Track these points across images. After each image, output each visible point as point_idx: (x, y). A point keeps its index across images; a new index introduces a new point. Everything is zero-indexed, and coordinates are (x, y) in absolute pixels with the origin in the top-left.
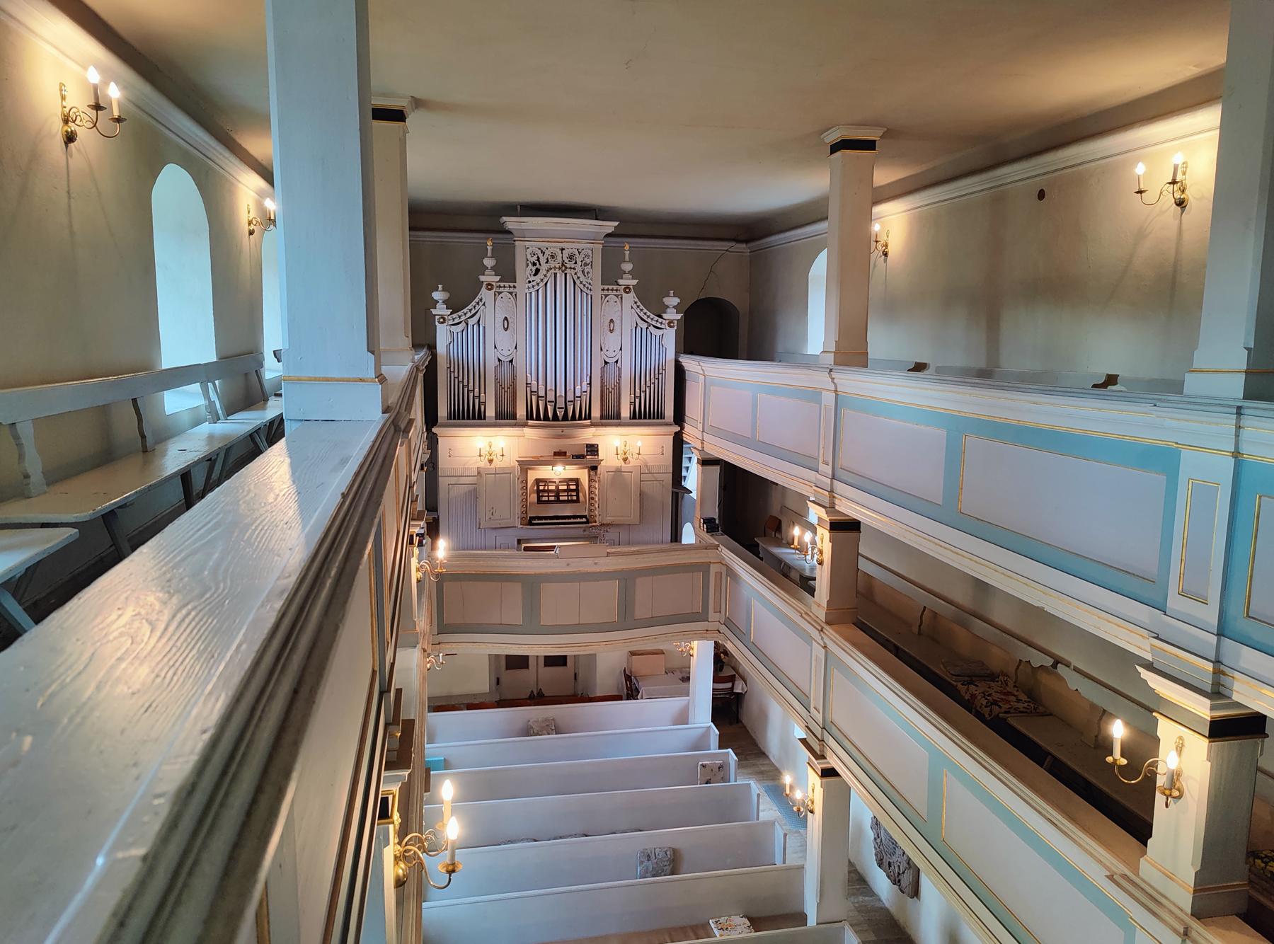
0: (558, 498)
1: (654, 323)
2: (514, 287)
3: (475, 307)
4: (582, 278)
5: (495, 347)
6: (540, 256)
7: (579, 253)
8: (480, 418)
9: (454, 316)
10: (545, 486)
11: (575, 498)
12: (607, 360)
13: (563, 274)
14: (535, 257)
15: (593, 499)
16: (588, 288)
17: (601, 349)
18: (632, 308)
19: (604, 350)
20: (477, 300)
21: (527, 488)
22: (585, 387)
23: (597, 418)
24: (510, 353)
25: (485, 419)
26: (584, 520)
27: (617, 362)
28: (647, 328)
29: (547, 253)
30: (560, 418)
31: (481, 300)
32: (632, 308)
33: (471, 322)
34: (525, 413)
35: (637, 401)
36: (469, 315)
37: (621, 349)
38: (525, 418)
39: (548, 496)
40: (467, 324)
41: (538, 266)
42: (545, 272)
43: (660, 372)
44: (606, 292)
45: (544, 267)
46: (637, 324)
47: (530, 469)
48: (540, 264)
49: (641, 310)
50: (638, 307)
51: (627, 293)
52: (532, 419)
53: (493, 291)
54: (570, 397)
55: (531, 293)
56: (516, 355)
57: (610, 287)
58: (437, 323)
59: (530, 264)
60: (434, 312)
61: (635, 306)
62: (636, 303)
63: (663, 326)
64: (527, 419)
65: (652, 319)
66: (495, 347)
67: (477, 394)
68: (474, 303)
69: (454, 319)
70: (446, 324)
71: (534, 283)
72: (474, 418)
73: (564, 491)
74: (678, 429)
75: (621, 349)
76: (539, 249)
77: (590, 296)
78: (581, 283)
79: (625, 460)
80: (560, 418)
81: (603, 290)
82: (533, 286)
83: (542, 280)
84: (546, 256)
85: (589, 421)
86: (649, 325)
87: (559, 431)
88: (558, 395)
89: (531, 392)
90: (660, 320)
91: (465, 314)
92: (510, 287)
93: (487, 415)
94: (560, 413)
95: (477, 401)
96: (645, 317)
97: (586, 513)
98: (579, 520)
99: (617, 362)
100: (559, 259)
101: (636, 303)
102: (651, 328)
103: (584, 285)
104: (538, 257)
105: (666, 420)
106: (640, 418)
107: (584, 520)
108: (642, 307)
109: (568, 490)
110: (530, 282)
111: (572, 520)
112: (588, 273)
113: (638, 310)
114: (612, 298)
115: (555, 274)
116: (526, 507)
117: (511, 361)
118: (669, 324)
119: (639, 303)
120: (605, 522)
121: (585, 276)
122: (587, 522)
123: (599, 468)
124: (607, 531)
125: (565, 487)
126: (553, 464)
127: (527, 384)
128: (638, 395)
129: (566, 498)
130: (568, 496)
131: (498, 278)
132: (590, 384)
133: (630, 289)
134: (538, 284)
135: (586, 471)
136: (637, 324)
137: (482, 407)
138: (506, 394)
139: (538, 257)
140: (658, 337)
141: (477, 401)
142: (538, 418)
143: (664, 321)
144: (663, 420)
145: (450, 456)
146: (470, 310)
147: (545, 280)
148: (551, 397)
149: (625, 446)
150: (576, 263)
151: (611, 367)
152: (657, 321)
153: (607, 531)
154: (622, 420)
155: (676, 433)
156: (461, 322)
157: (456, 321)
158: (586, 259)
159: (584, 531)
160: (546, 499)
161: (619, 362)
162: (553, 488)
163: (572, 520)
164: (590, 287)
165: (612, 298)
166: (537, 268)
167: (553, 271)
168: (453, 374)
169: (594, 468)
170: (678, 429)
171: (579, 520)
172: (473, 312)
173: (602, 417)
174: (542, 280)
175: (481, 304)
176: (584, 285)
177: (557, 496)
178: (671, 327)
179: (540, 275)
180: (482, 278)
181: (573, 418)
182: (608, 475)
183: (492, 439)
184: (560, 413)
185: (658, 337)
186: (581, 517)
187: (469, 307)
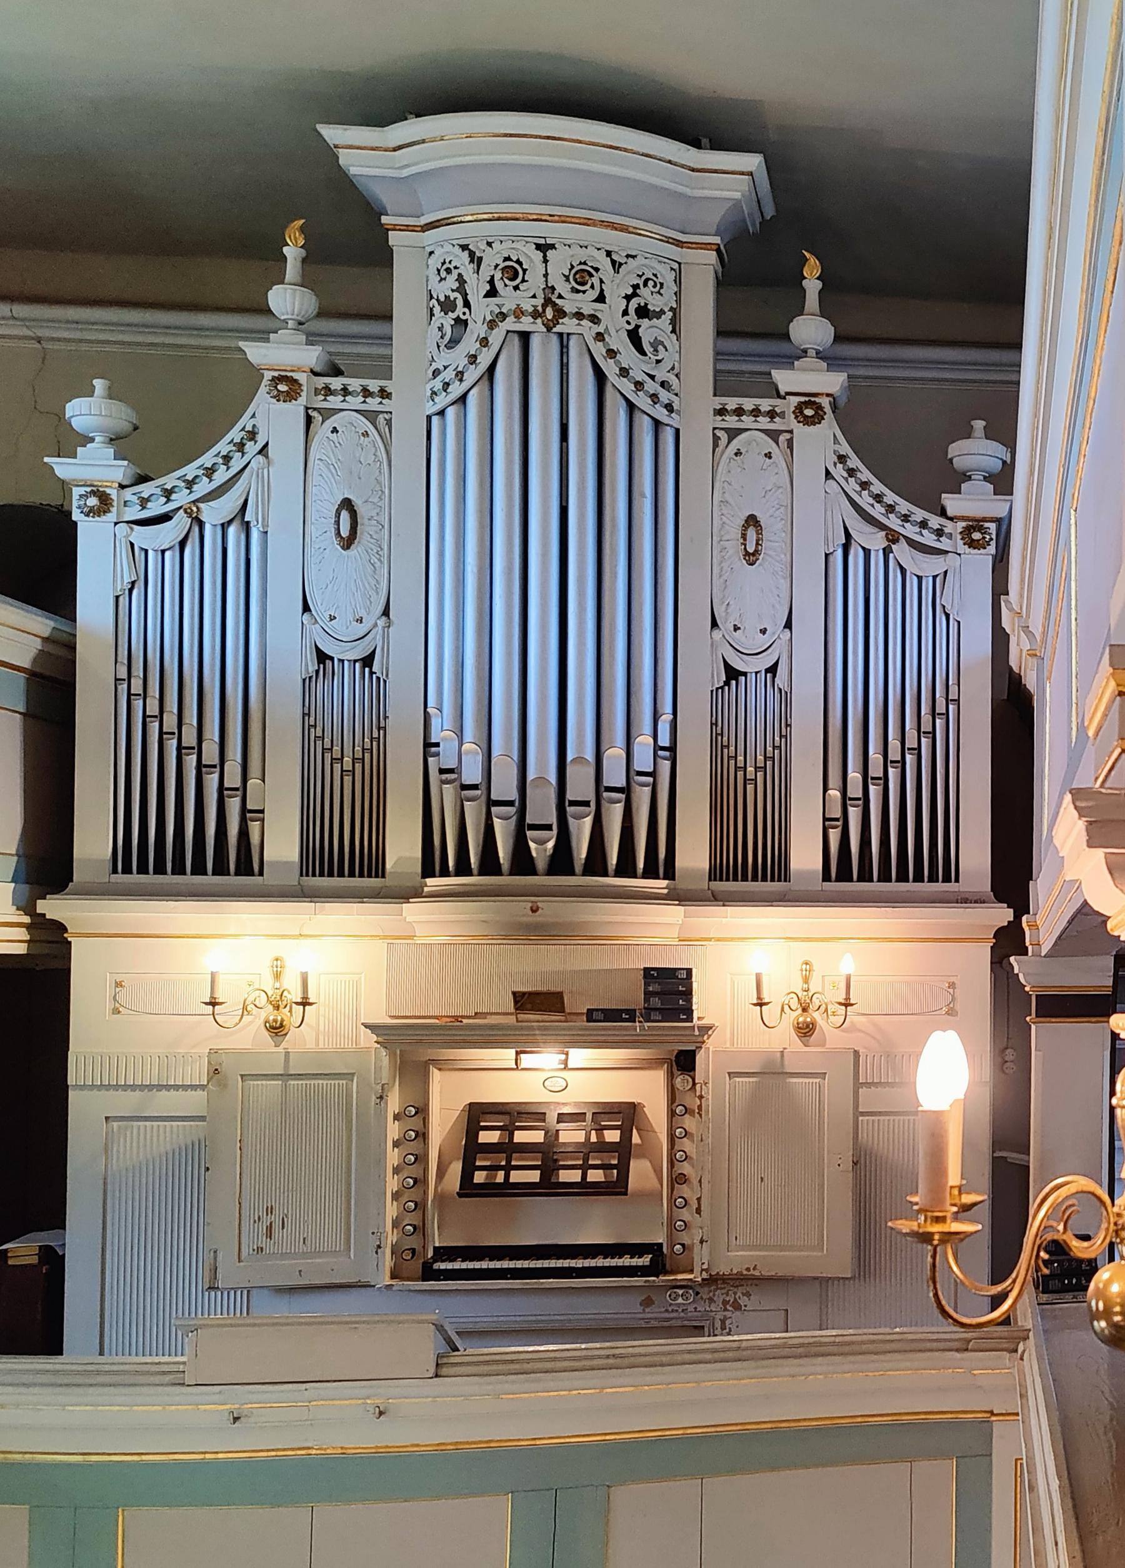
1: (910, 531)
2: (384, 394)
3: (227, 459)
4: (628, 355)
5: (306, 608)
6: (468, 271)
7: (616, 266)
8: (245, 867)
9: (146, 489)
12: (738, 664)
13: (555, 340)
14: (451, 282)
15: (681, 1179)
16: (654, 397)
17: (714, 624)
18: (828, 473)
19: (726, 625)
20: (235, 434)
21: (422, 1135)
22: (643, 760)
23: (691, 874)
24: (362, 629)
25: (261, 874)
26: (645, 1260)
27: (773, 670)
28: (887, 551)
29: (492, 258)
30: (541, 864)
31: (252, 435)
32: (828, 473)
33: (213, 514)
34: (419, 854)
35: (854, 814)
36: (203, 487)
37: (788, 625)
38: (418, 868)
40: (201, 524)
41: (460, 309)
42: (482, 331)
43: (940, 708)
44: (732, 421)
45: (482, 308)
46: (848, 535)
47: (442, 1065)
48: (467, 304)
49: (865, 485)
50: (851, 472)
51: (808, 421)
52: (445, 873)
53: (295, 410)
54: (580, 786)
55: (442, 413)
56: (386, 638)
57: (748, 404)
58: (76, 516)
59: (437, 309)
60: (63, 468)
61: (839, 472)
62: (842, 459)
63: (944, 544)
64: (428, 871)
65: (906, 518)
66: (306, 608)
67: (233, 778)
68: (223, 447)
69: (144, 502)
70: (111, 517)
71: (448, 375)
72: (221, 869)
74: (1003, 915)
75: (788, 625)
76: (464, 247)
77: (668, 437)
78: (624, 372)
79: (806, 1031)
80: (541, 864)
81: (721, 412)
82: (446, 385)
83: (473, 359)
84: (486, 271)
85: (665, 883)
86: (893, 537)
87: (522, 906)
88: (531, 775)
89: (442, 771)
90: (935, 521)
91: (190, 484)
92: (366, 393)
93: (265, 858)
94: (542, 848)
95: (233, 806)
96: (877, 511)
97: (661, 1239)
98: (626, 1261)
99: (773, 670)
100: (535, 282)
101: (842, 459)
102: (901, 551)
103: (639, 385)
104: (461, 279)
105: (965, 885)
106: (865, 876)
107: (645, 1260)
108: (865, 475)
109: (588, 1149)
110: (436, 373)
111: (599, 1262)
112: (656, 344)
113: (852, 486)
114: (754, 441)
115: (525, 337)
116: (420, 1206)
117: (368, 661)
118: (967, 532)
119: (854, 462)
120: (723, 1269)
121: (643, 353)
122: (657, 1267)
123: (700, 1058)
124: (737, 1307)
125: (580, 1137)
126: (522, 1042)
127: (428, 745)
128: (855, 790)
129: (575, 1176)
130: (585, 1168)
131: (311, 356)
132: (672, 749)
133: (819, 408)
134: (460, 375)
135: (657, 1078)
136: (848, 535)
137: (254, 827)
138: (348, 779)
139: (461, 279)
140: (927, 584)
141: (233, 806)
142: (463, 868)
143: (949, 527)
144: (951, 887)
145: (116, 1011)
146: (210, 472)
147: (485, 360)
148: (505, 786)
149: (806, 980)
150: (601, 298)
151: (753, 690)
152: (924, 524)
153: (737, 1307)
154: (794, 884)
155: (1000, 933)
156: (165, 518)
157: (156, 508)
158: (643, 291)
159: (648, 1302)
160: (500, 1177)
161: (782, 670)
162: (537, 1137)
163: (599, 1262)
164: (665, 396)
165: (754, 441)
166: (458, 320)
167: (510, 324)
168: (138, 704)
169: (685, 1062)
170: (1003, 915)
171: (626, 1261)
172: (221, 476)
173: (716, 873)
174: (473, 359)
175: (251, 448)
176: (639, 385)
177: (549, 1168)
178: (972, 544)
179: (469, 344)
180: (255, 352)
181: (596, 864)
182: (733, 1088)
183: (282, 948)
184: (542, 848)
185: (927, 584)
186: (636, 1250)
187: (207, 459)
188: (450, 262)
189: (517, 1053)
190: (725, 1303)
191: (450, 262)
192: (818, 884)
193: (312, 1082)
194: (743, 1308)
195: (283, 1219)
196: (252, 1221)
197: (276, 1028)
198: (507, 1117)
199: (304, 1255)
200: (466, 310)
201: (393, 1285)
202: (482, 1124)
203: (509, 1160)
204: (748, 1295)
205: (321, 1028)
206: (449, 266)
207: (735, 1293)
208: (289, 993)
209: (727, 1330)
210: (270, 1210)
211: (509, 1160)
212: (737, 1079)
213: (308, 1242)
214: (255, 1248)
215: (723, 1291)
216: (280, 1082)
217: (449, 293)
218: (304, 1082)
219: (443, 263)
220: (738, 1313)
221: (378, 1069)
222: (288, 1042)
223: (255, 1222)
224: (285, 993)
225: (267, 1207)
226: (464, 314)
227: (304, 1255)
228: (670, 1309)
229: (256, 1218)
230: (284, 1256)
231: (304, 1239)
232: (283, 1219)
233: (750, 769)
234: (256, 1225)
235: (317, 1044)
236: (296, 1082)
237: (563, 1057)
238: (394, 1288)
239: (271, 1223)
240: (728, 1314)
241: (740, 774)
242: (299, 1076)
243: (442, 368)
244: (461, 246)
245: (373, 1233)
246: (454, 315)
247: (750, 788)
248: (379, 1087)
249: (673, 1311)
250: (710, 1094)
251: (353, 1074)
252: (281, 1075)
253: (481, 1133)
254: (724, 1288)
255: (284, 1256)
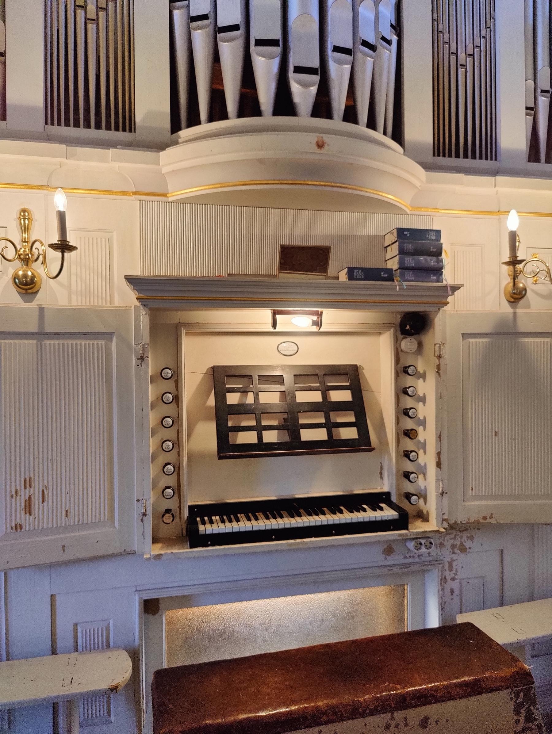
0: (295, 435)
10: (244, 392)
11: (350, 433)
21: (177, 399)
39: (259, 429)
73: (314, 407)
116: (178, 469)
125: (316, 397)
129: (321, 435)
132: (398, 28)
153: (463, 549)
159: (389, 550)
160: (250, 438)
189: (275, 314)
190: (453, 546)
192: (523, 162)
193: (70, 342)
194: (468, 550)
195: (43, 491)
196: (9, 497)
197: (26, 284)
198: (245, 380)
199: (67, 529)
201: (161, 555)
202: (227, 386)
203: (259, 421)
204: (471, 538)
205: (74, 287)
207: (461, 537)
208: (41, 243)
209: (454, 572)
210: (28, 483)
211: (259, 421)
212: (471, 340)
213: (71, 514)
214: (13, 525)
215: (452, 536)
216: (35, 342)
218: (61, 342)
220: (463, 555)
221: (138, 329)
222: (41, 298)
223: (12, 496)
224: (37, 245)
225: (25, 480)
227: (67, 529)
228: (408, 556)
229: (13, 493)
230: (44, 532)
231: (67, 512)
232: (43, 491)
233: (462, 56)
234: (13, 500)
235: (70, 300)
236: (52, 342)
237: (315, 318)
238: (164, 558)
239: (30, 497)
240: (455, 557)
241: (453, 58)
242: (56, 335)
245: (138, 501)
247: (461, 71)
248: (140, 348)
249: (410, 557)
250: (446, 353)
251: (111, 334)
252: (36, 333)
253: (228, 395)
254: (452, 533)
255: (44, 532)
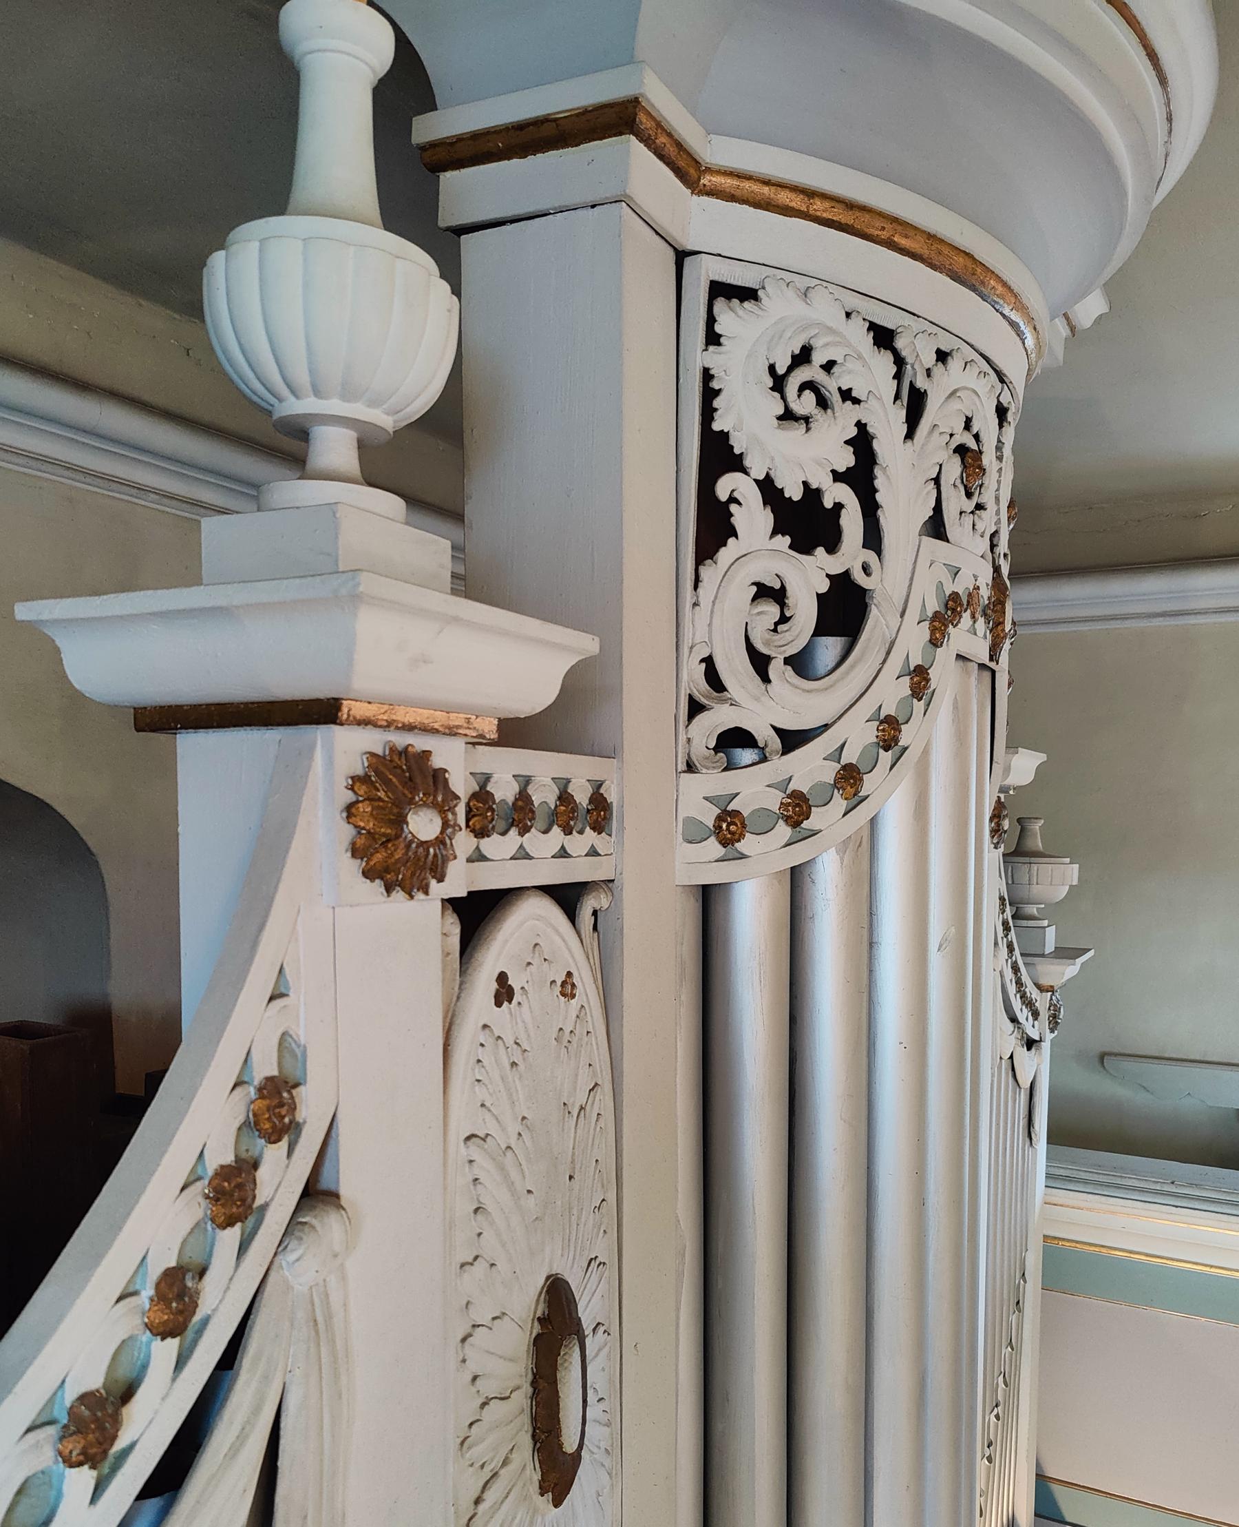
48: (873, 539)
76: (883, 337)
104: (862, 442)
139: (862, 442)
188: (829, 366)
191: (829, 366)
200: (870, 556)
206: (820, 377)
217: (822, 480)
219: (803, 357)
226: (866, 569)
243: (763, 734)
244: (873, 327)
246: (835, 565)
